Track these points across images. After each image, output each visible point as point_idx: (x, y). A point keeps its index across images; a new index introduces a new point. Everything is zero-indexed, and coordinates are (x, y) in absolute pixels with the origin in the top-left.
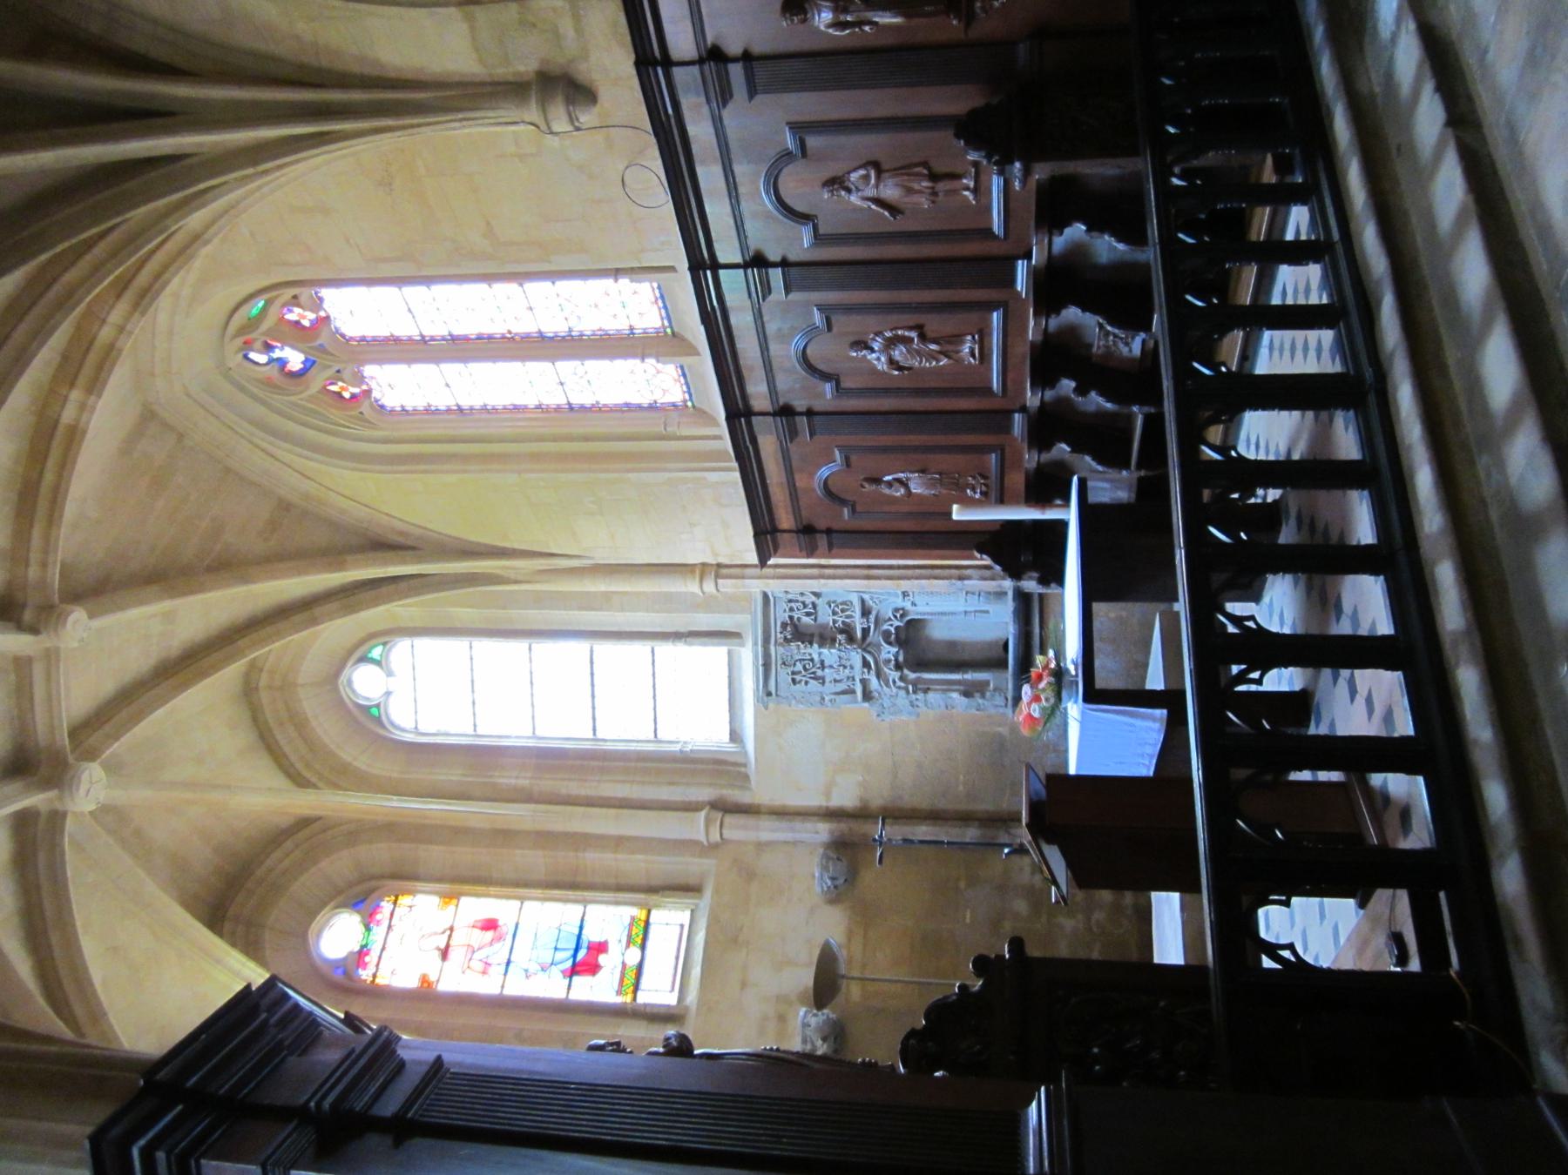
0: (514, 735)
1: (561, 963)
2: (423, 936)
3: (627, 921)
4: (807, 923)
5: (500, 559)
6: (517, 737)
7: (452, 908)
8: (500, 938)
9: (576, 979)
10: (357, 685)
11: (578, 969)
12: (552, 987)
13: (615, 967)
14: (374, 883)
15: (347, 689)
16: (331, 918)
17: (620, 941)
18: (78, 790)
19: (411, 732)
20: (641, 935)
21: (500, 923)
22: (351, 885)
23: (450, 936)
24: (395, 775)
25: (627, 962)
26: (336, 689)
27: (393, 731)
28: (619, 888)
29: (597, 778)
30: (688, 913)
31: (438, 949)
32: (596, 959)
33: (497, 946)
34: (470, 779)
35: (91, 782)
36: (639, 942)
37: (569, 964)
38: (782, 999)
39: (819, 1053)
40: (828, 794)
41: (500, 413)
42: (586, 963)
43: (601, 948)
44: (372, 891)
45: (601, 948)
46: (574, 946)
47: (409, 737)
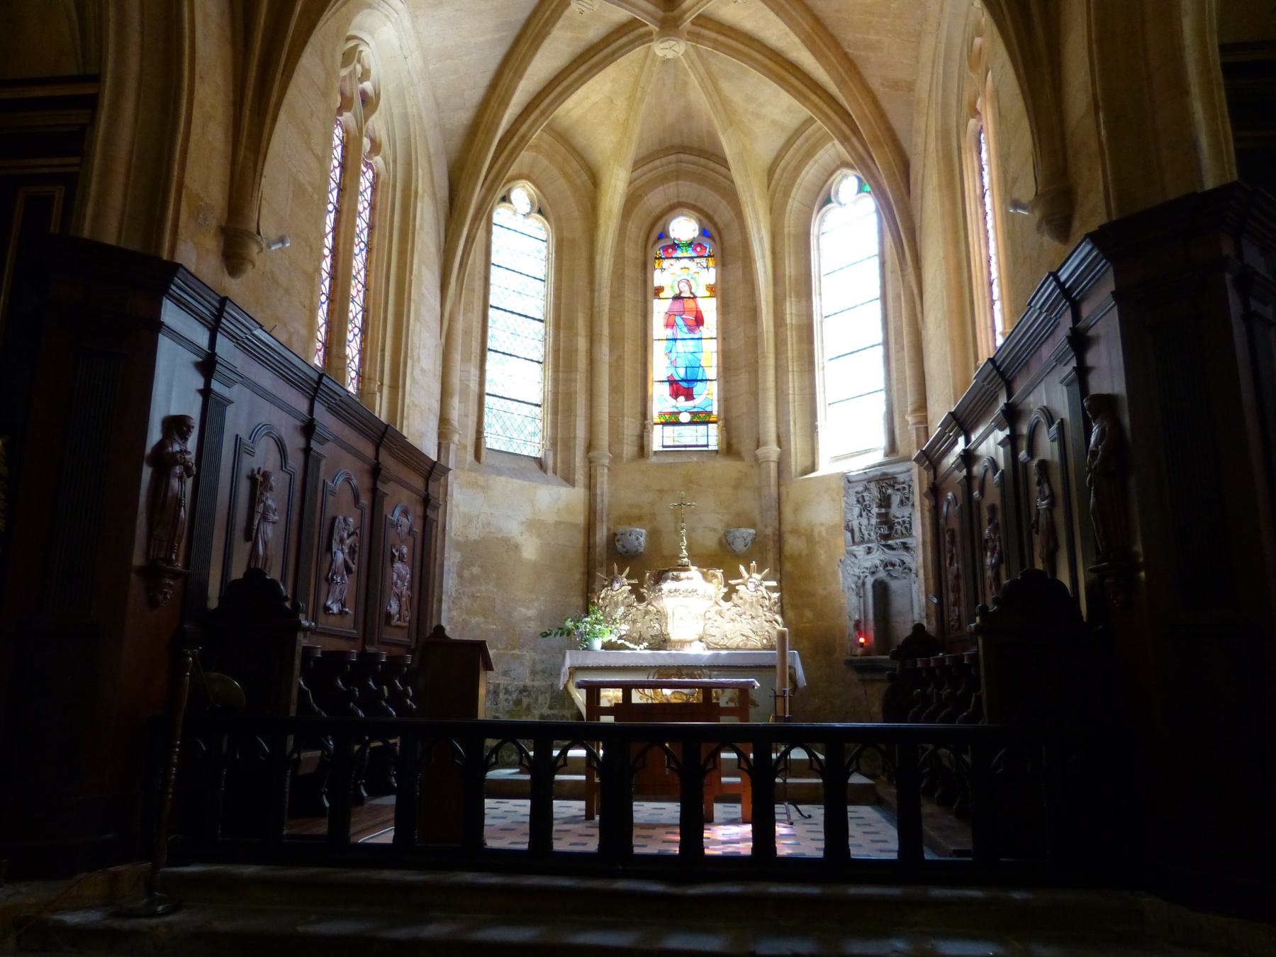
0: (822, 304)
1: (677, 373)
2: (688, 281)
3: (708, 409)
4: (705, 527)
5: (913, 261)
6: (821, 306)
7: (708, 294)
8: (691, 330)
9: (667, 386)
10: (845, 182)
11: (674, 386)
12: (661, 367)
13: (677, 408)
14: (717, 238)
15: (840, 176)
16: (693, 218)
17: (694, 407)
18: (662, 42)
19: (819, 231)
20: (700, 419)
21: (701, 328)
22: (715, 225)
23: (689, 298)
24: (786, 230)
25: (681, 414)
26: (838, 168)
27: (818, 218)
28: (726, 400)
29: (795, 369)
30: (716, 448)
31: (681, 292)
32: (682, 395)
33: (685, 329)
34: (787, 282)
35: (671, 48)
36: (695, 420)
37: (677, 378)
38: (653, 515)
39: (617, 543)
40: (792, 532)
41: (368, 305)
42: (681, 388)
43: (689, 396)
44: (714, 240)
45: (689, 396)
46: (689, 378)
47: (814, 230)
